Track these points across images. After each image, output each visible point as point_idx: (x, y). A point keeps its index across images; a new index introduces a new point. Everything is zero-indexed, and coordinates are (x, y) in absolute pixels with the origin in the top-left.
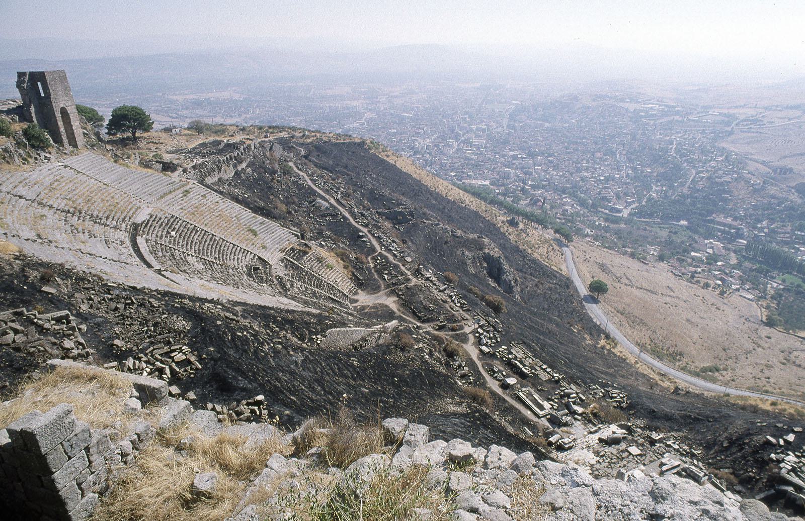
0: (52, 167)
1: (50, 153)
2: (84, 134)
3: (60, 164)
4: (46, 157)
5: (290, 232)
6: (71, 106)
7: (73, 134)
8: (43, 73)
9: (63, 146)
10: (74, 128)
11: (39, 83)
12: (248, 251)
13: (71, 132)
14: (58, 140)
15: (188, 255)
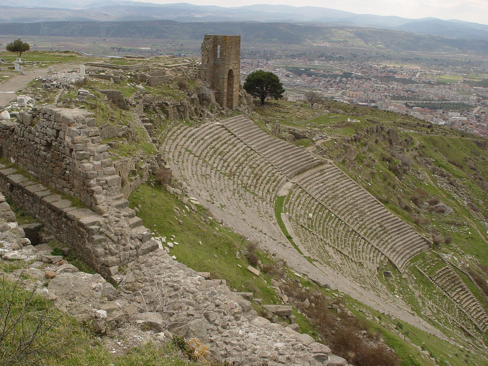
0: (212, 125)
2: (240, 96)
3: (218, 123)
4: (208, 115)
5: (422, 238)
6: (237, 69)
7: (232, 95)
8: (225, 37)
10: (234, 89)
11: (219, 46)
12: (379, 251)
13: (231, 93)
15: (326, 244)
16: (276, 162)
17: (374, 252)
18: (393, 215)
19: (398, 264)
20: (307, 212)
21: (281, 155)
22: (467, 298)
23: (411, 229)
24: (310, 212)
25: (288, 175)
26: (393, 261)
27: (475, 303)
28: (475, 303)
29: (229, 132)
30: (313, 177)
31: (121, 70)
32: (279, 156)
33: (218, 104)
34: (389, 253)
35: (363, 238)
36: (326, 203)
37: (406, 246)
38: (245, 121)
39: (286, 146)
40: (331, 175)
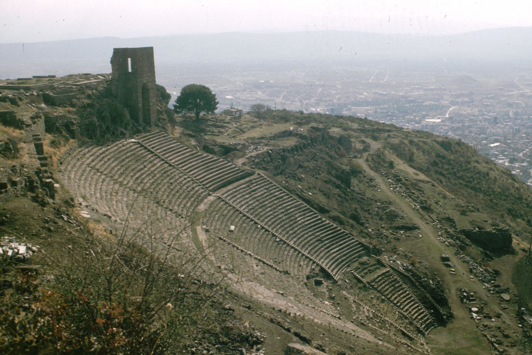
1: (126, 129)
3: (133, 140)
5: (360, 243)
7: (149, 110)
10: (151, 104)
14: (135, 118)
16: (195, 177)
17: (304, 260)
18: (327, 222)
19: (332, 271)
20: (229, 224)
21: (203, 169)
22: (409, 301)
23: (347, 234)
24: (232, 224)
25: (210, 189)
26: (326, 268)
29: (146, 148)
30: (238, 188)
31: (22, 91)
32: (201, 170)
34: (322, 260)
35: (292, 247)
36: (251, 214)
37: (342, 252)
38: (164, 137)
39: (209, 159)
40: (259, 186)
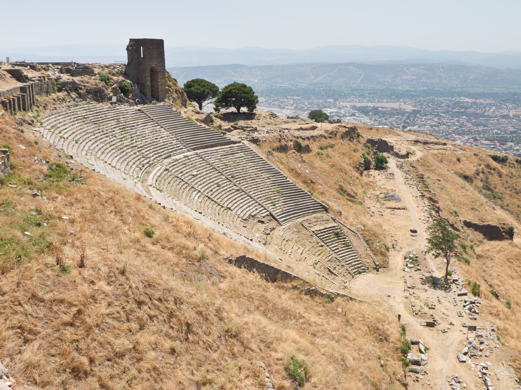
7: (157, 88)
9: (146, 96)
10: (159, 84)
27: (355, 254)
28: (355, 254)
33: (142, 95)
